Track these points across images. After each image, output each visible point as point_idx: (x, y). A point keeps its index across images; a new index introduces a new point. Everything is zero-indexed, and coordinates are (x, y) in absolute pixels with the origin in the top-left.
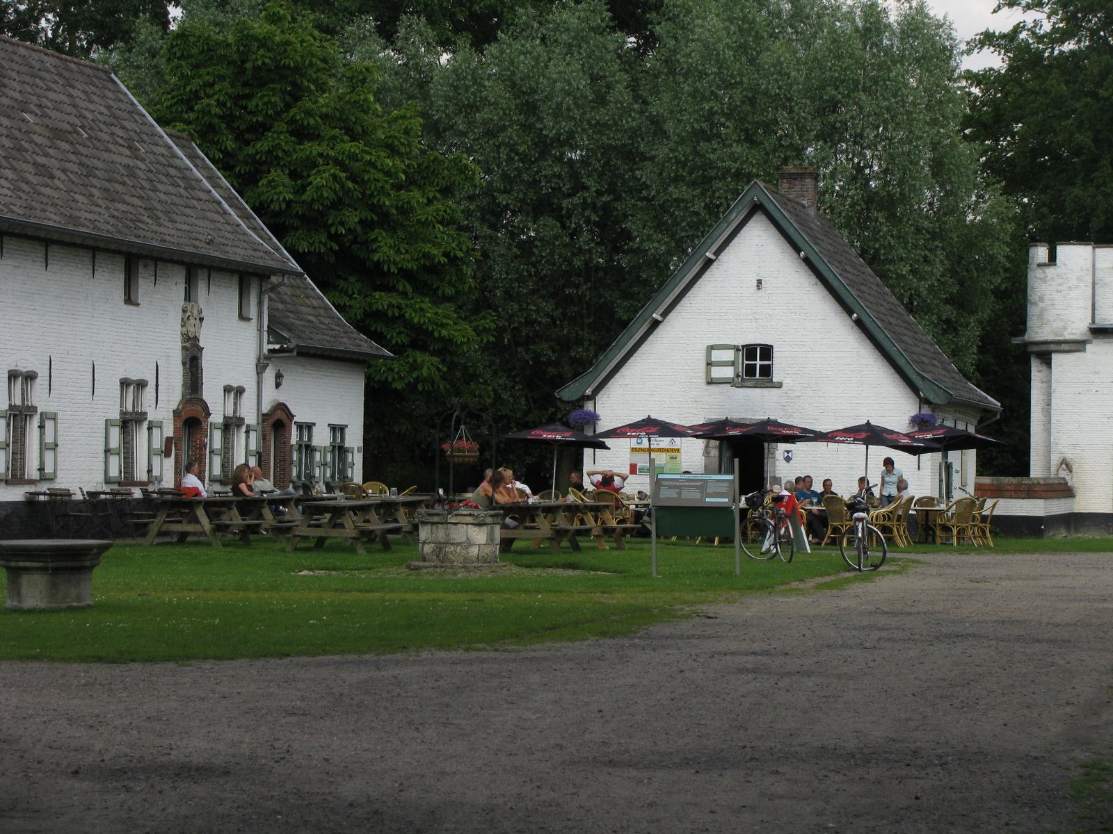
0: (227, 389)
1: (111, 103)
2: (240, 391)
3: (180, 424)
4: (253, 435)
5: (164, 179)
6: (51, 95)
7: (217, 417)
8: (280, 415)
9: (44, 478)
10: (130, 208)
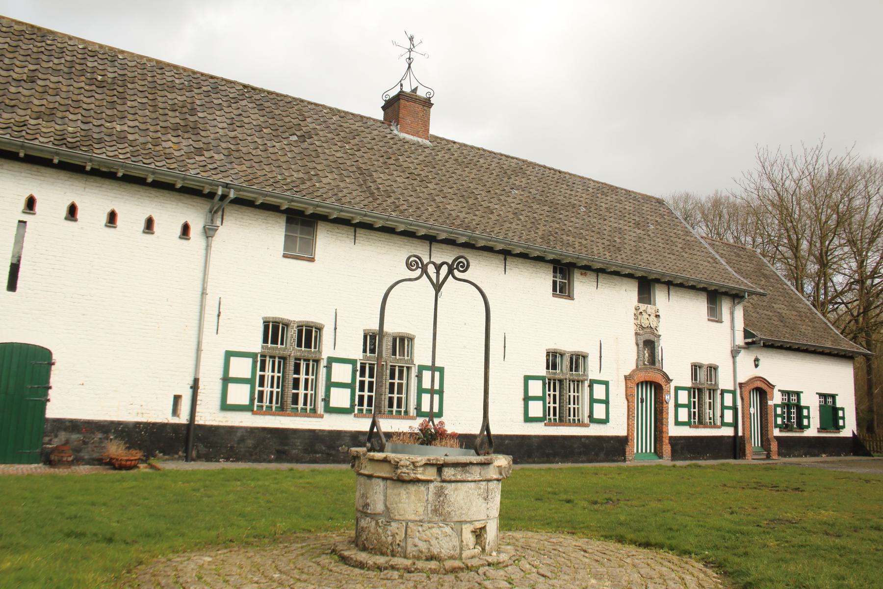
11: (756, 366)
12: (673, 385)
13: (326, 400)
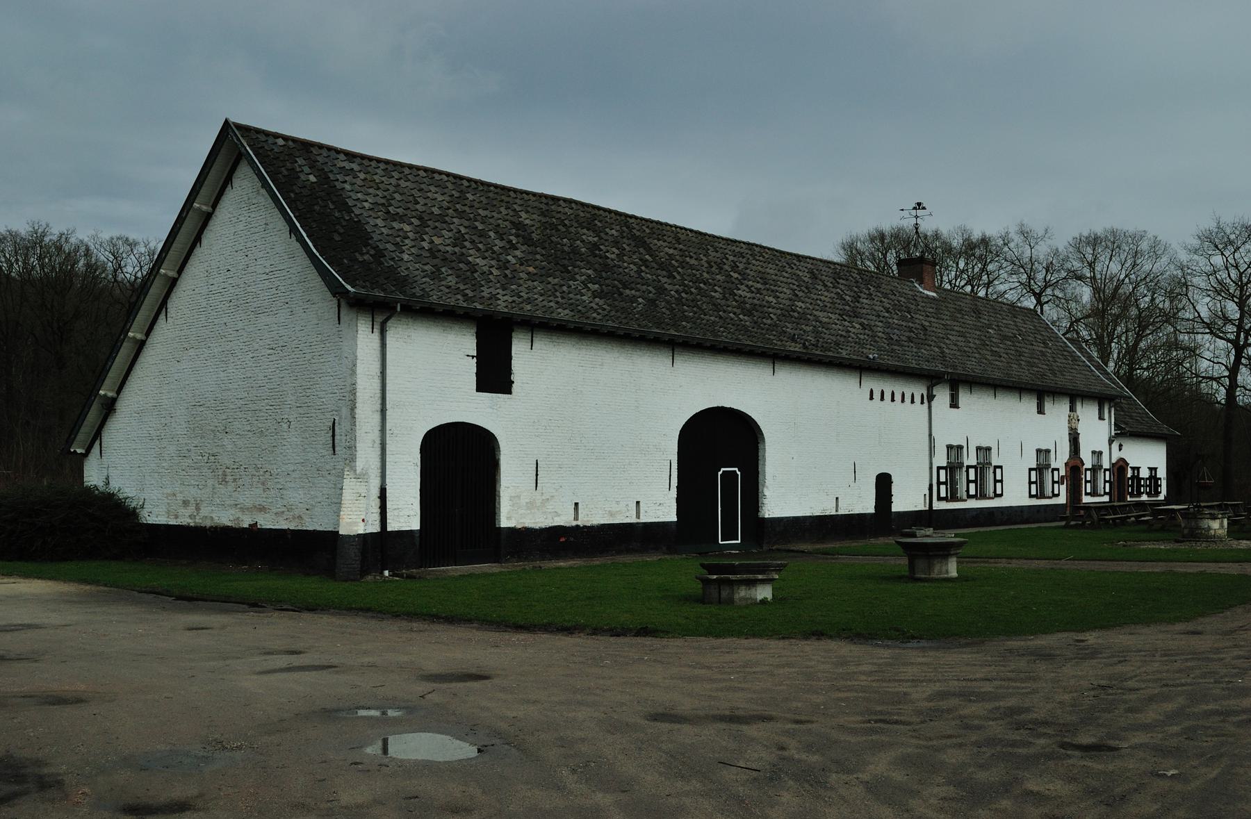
0: (1094, 452)
1: (1036, 324)
2: (1100, 453)
3: (1068, 469)
4: (1107, 473)
5: (1061, 357)
6: (1004, 321)
7: (1088, 465)
8: (1121, 463)
9: (997, 495)
10: (1041, 370)
11: (1120, 450)
12: (1084, 467)
13: (968, 491)
